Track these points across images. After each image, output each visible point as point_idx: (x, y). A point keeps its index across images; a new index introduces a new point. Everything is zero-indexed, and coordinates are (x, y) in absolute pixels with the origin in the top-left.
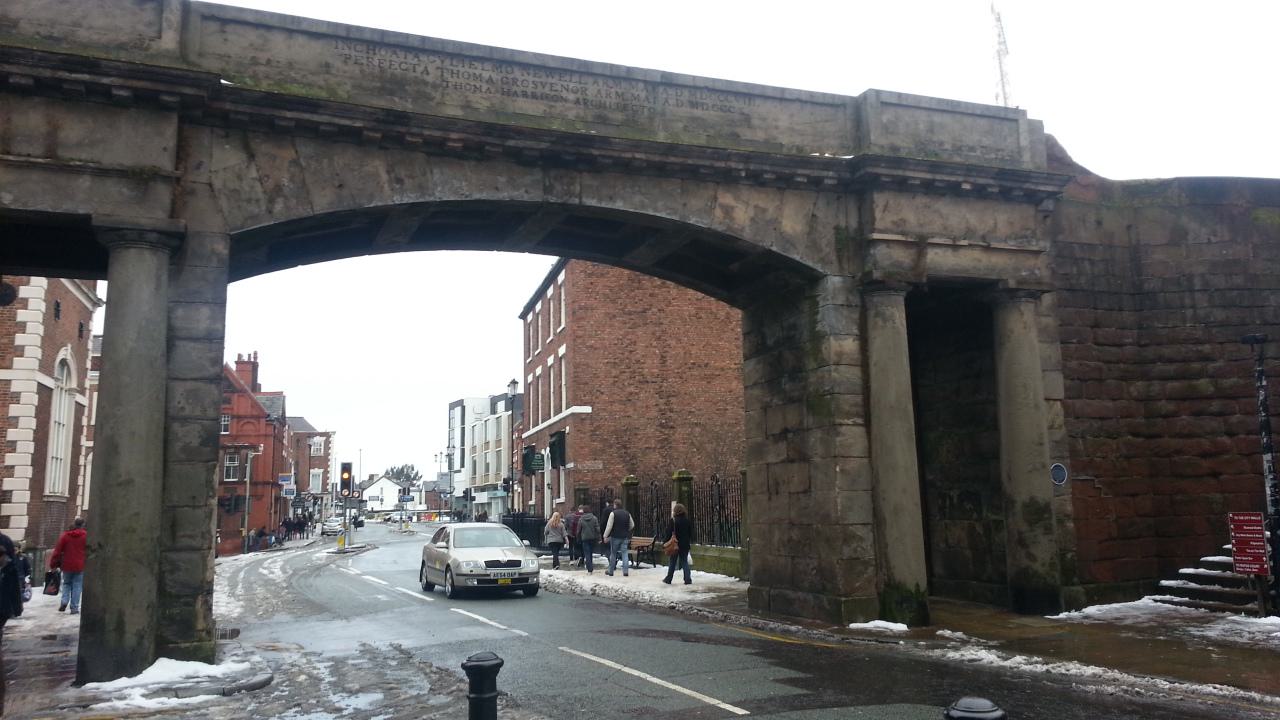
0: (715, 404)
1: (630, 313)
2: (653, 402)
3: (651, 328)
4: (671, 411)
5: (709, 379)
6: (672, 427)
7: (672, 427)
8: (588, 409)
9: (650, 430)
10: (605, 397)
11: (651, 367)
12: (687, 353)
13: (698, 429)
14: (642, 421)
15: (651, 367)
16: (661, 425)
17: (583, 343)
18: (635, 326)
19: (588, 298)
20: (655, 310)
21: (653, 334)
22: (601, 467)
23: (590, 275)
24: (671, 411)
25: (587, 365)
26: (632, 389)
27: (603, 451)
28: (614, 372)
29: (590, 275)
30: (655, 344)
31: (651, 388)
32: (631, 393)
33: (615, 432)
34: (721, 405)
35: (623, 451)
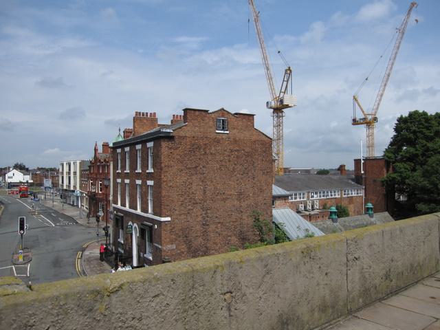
0: (227, 212)
1: (189, 168)
2: (199, 213)
3: (199, 176)
4: (208, 217)
5: (224, 200)
6: (208, 225)
7: (208, 225)
8: (169, 219)
9: (198, 227)
10: (177, 212)
11: (199, 196)
12: (216, 188)
13: (219, 225)
14: (195, 223)
15: (199, 196)
16: (203, 224)
17: (167, 185)
18: (192, 175)
19: (169, 161)
20: (201, 167)
21: (200, 179)
22: (175, 247)
23: (171, 148)
24: (208, 217)
25: (169, 197)
26: (190, 207)
27: (176, 240)
28: (182, 199)
29: (171, 148)
30: (201, 183)
31: (199, 206)
32: (189, 210)
33: (181, 230)
34: (230, 213)
35: (185, 239)
